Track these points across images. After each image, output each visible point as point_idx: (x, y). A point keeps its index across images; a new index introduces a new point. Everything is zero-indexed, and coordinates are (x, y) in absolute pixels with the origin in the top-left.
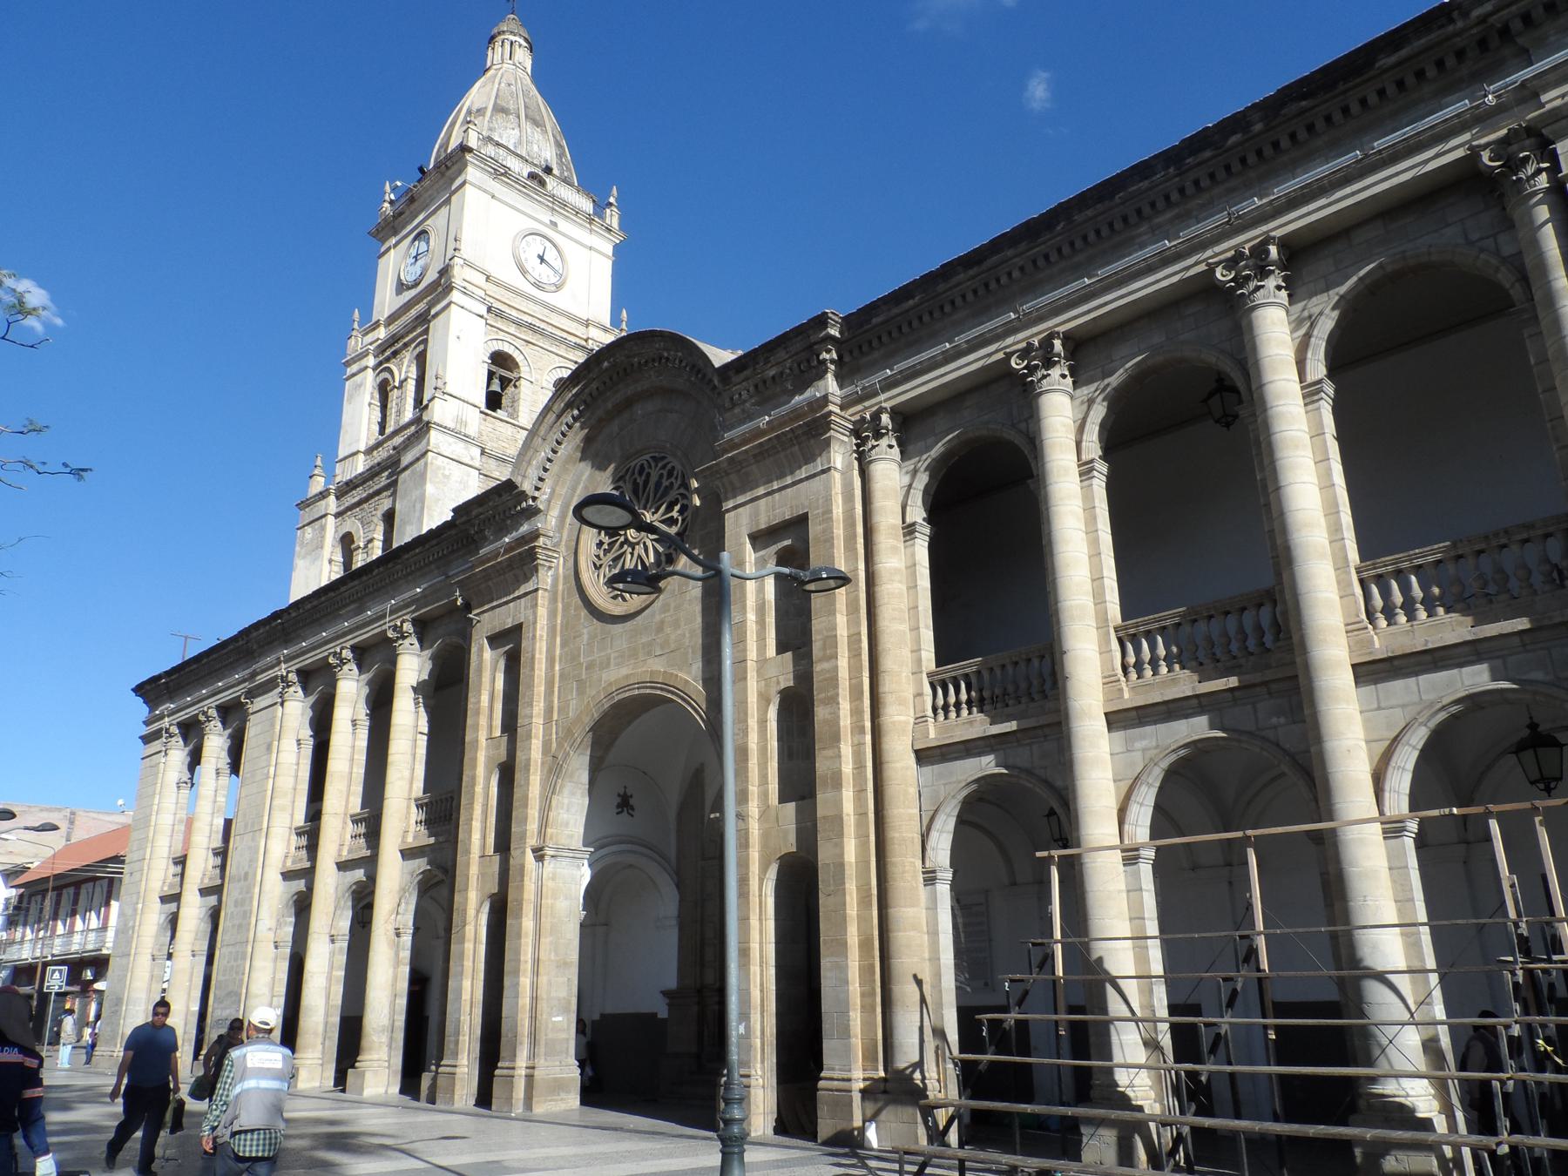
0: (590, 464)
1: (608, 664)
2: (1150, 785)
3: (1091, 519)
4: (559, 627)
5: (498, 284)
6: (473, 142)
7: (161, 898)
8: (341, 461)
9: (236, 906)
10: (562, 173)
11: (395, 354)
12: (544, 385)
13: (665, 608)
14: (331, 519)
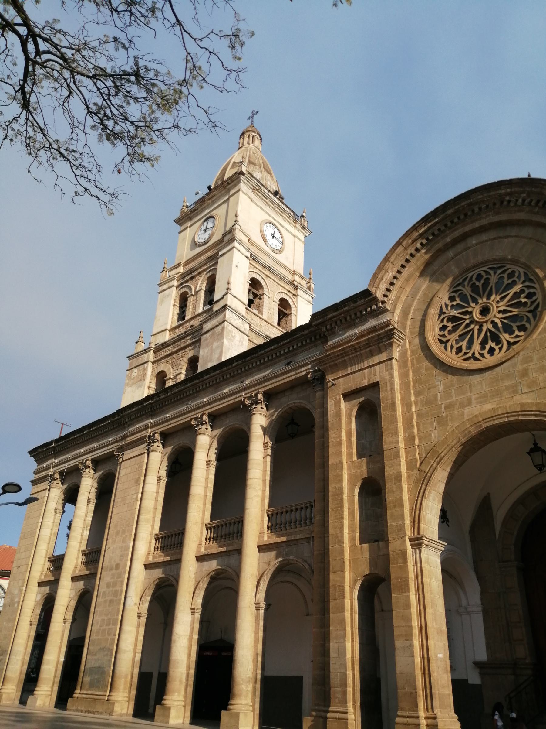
0: (428, 278)
1: (469, 403)
4: (411, 383)
5: (253, 244)
6: (244, 169)
8: (154, 335)
11: (192, 278)
12: (275, 300)
13: (528, 360)
14: (150, 364)
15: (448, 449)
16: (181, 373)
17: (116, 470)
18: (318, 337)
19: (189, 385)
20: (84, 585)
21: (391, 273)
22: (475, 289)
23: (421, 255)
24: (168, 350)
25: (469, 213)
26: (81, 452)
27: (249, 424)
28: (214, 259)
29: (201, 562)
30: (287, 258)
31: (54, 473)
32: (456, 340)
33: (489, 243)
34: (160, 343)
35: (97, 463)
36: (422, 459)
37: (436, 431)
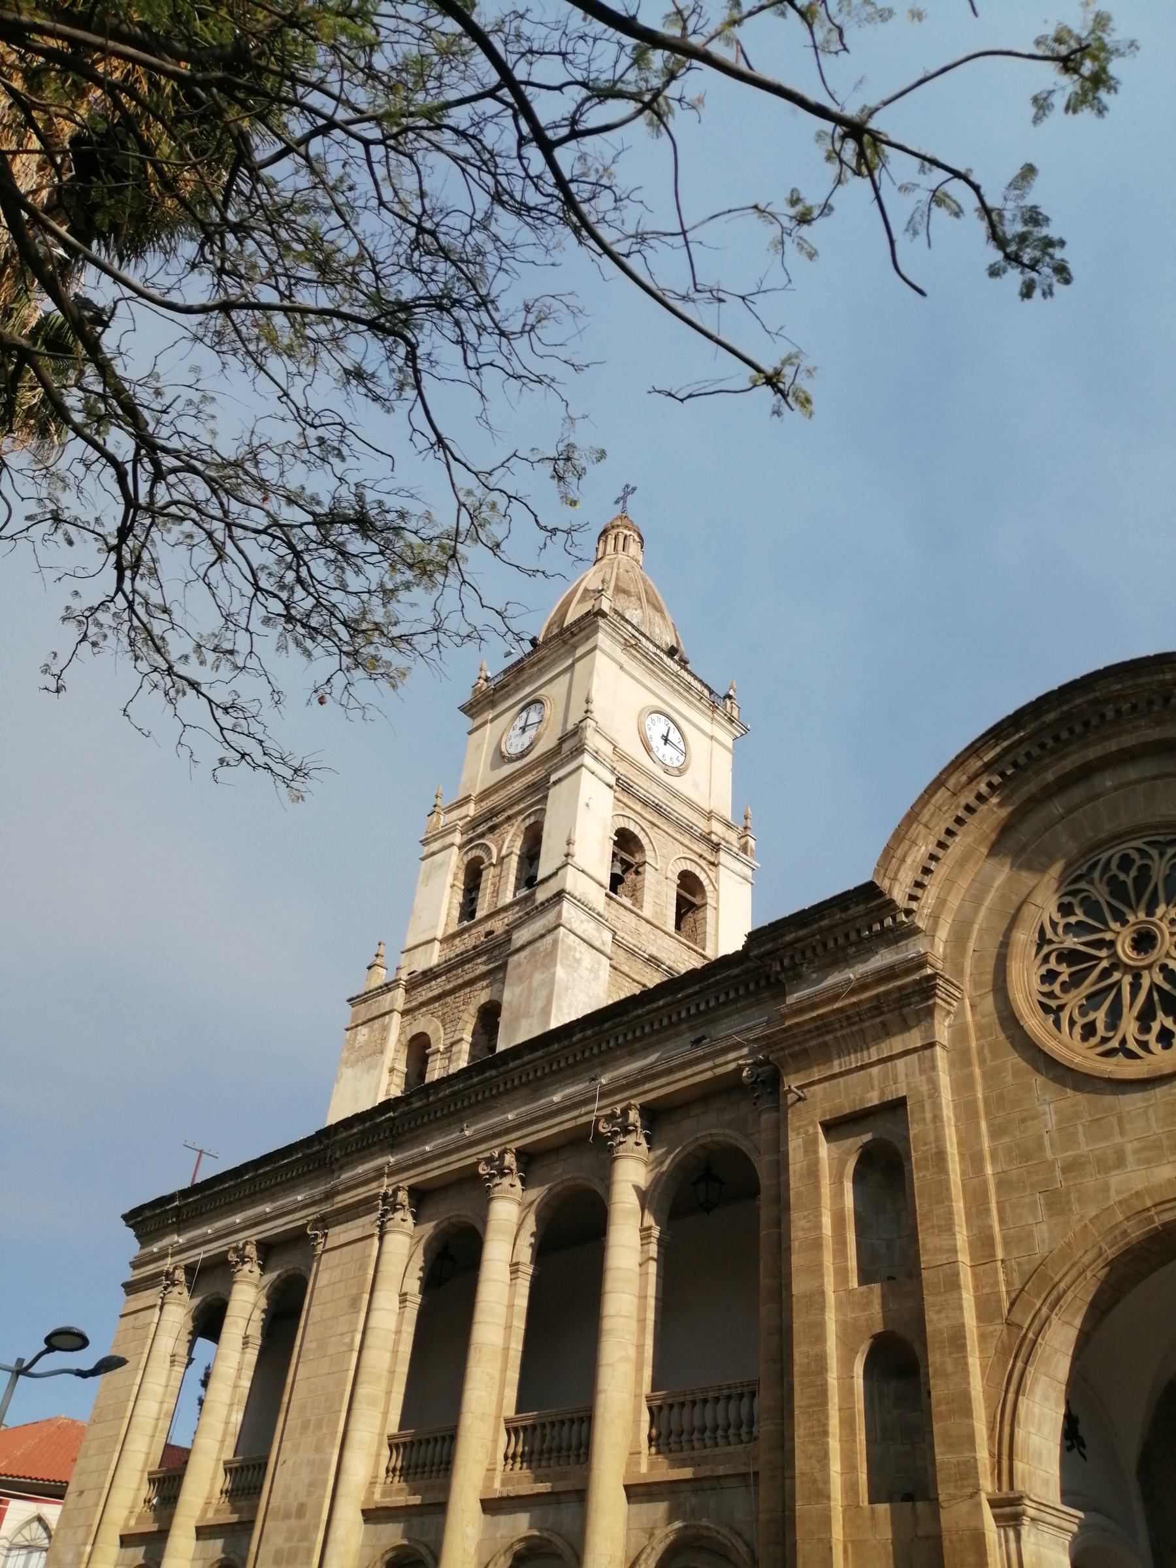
0: (1008, 861)
5: (623, 758)
6: (606, 606)
7: (122, 1538)
8: (409, 950)
11: (492, 829)
12: (669, 875)
14: (396, 1017)
15: (1074, 1272)
16: (462, 1039)
17: (310, 1270)
18: (763, 983)
19: (475, 1080)
20: (224, 1551)
21: (923, 848)
22: (1117, 889)
23: (991, 810)
25: (1094, 721)
26: (234, 1224)
27: (606, 1178)
28: (540, 788)
29: (493, 1515)
30: (696, 785)
31: (175, 1268)
32: (1081, 1006)
33: (1142, 786)
34: (420, 970)
35: (268, 1250)
36: (1014, 1295)
37: (1044, 1227)
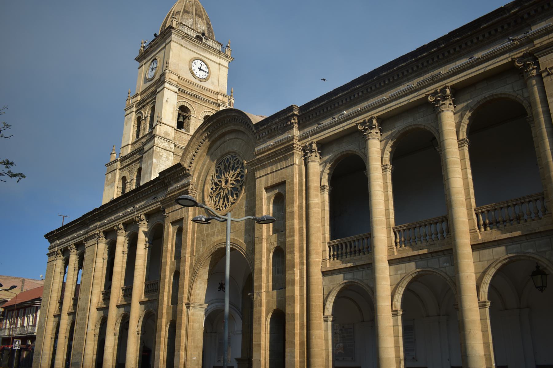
1: (214, 234)
2: (402, 287)
3: (386, 187)
5: (183, 79)
6: (174, 25)
8: (122, 148)
9: (80, 320)
10: (209, 35)
11: (143, 106)
12: (200, 118)
14: (118, 171)
16: (133, 179)
22: (225, 168)
23: (206, 143)
24: (128, 161)
30: (213, 83)
37: (202, 248)
